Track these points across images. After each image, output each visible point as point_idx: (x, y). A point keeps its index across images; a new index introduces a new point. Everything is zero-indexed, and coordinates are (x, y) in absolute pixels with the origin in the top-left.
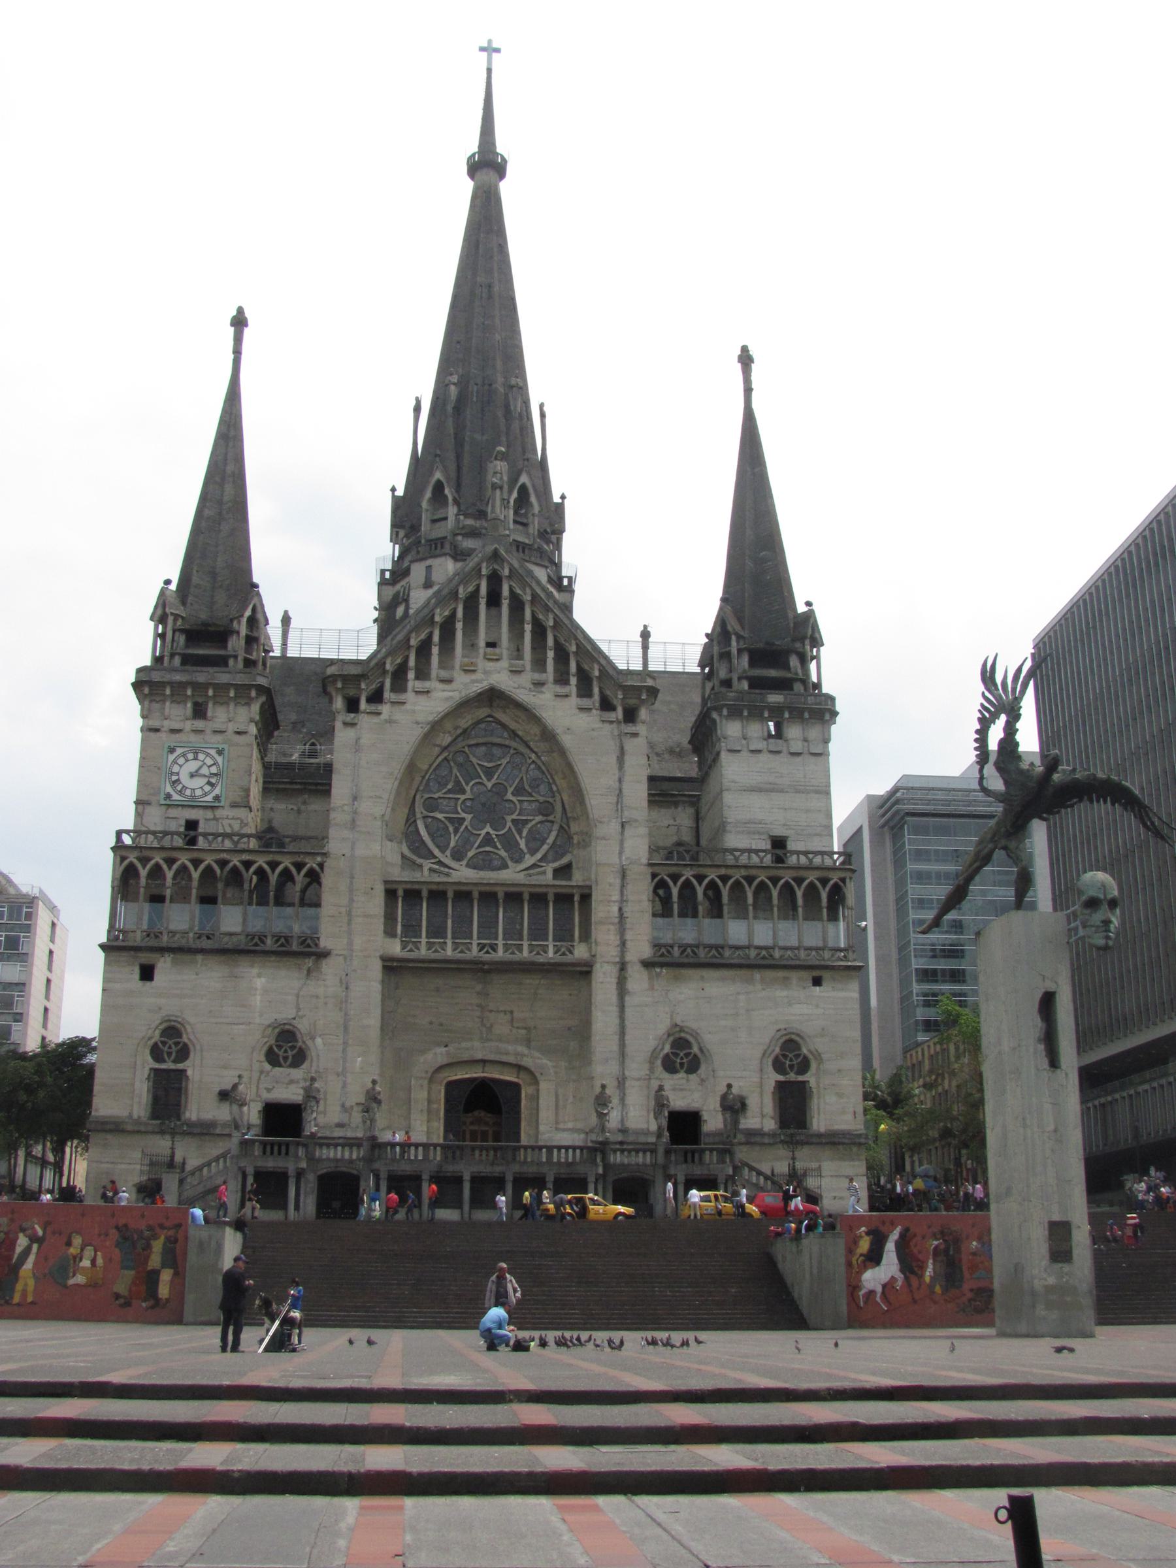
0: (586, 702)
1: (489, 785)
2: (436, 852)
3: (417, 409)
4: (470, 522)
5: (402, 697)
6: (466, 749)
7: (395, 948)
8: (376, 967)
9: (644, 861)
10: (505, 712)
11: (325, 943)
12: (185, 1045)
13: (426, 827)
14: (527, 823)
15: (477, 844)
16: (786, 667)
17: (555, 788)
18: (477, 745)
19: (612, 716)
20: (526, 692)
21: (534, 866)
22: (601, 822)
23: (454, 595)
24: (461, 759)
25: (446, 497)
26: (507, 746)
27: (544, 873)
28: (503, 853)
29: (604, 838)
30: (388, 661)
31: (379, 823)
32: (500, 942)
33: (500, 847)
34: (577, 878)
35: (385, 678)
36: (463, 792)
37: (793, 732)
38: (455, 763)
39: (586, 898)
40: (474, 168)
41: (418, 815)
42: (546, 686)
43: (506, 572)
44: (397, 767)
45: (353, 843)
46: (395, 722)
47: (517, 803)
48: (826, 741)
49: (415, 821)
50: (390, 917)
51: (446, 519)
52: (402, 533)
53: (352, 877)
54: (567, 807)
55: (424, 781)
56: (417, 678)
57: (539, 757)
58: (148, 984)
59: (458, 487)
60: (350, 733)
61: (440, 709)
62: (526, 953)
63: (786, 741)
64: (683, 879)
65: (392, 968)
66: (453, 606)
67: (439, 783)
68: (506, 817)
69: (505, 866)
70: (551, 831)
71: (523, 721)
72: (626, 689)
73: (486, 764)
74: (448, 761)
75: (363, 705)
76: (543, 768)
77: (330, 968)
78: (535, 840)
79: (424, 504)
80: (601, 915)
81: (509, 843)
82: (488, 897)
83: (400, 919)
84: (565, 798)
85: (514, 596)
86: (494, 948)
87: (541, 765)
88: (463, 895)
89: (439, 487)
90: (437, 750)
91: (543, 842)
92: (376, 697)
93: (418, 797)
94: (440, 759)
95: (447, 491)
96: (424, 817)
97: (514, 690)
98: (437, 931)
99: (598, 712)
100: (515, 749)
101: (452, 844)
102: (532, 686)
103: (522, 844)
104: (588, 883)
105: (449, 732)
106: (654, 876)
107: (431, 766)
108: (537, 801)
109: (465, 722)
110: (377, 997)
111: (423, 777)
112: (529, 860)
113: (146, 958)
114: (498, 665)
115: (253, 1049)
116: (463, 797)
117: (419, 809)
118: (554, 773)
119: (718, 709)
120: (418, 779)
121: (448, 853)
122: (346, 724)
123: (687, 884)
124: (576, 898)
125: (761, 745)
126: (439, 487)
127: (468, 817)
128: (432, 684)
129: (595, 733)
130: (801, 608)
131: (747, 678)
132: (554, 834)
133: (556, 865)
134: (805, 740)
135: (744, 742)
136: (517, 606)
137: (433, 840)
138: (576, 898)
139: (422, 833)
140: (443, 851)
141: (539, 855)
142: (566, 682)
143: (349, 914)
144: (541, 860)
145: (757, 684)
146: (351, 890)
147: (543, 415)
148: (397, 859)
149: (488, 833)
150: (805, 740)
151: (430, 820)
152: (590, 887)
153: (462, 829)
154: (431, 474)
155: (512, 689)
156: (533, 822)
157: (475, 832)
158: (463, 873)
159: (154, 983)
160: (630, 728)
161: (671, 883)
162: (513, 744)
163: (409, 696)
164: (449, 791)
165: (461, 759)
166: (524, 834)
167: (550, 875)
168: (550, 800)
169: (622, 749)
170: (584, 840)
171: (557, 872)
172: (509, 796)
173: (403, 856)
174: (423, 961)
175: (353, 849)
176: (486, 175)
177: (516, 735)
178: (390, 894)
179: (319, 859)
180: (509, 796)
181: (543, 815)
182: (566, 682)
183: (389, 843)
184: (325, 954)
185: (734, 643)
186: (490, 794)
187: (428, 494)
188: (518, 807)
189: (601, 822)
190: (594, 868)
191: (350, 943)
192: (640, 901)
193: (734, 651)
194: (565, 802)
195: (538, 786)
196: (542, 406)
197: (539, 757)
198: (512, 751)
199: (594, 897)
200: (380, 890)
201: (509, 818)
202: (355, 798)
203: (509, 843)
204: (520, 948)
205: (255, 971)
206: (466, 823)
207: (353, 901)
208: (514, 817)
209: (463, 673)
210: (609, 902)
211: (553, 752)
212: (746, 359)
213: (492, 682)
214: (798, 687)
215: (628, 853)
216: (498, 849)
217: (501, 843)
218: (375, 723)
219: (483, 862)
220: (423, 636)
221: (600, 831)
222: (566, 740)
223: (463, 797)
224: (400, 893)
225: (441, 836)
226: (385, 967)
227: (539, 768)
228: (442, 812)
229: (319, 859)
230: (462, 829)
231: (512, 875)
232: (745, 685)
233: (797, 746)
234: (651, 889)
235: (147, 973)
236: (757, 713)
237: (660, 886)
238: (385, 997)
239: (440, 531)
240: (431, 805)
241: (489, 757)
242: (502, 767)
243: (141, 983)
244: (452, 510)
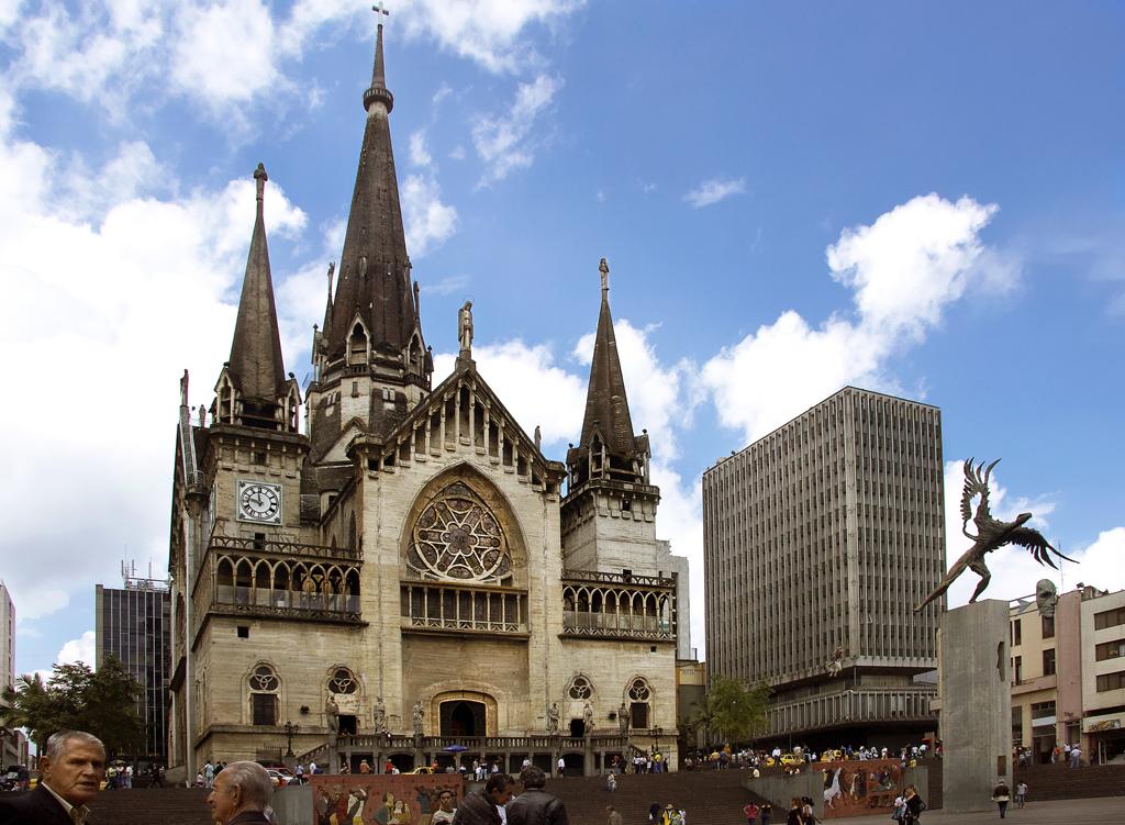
0: (520, 477)
1: (460, 525)
2: (428, 565)
3: (331, 272)
4: (380, 356)
5: (407, 463)
7: (409, 623)
8: (398, 634)
11: (364, 618)
12: (274, 679)
16: (632, 470)
19: (540, 488)
21: (489, 577)
23: (441, 397)
24: (441, 508)
25: (365, 336)
27: (496, 581)
28: (469, 568)
30: (399, 438)
32: (474, 622)
34: (516, 585)
36: (444, 529)
37: (636, 507)
39: (524, 597)
40: (368, 102)
44: (406, 509)
48: (654, 514)
50: (404, 605)
51: (365, 351)
52: (325, 359)
56: (417, 451)
58: (245, 640)
59: (371, 330)
60: (374, 484)
62: (489, 629)
63: (632, 512)
65: (407, 635)
69: (471, 576)
72: (548, 471)
77: (368, 634)
78: (490, 562)
79: (348, 340)
81: (474, 563)
82: (465, 594)
85: (477, 404)
86: (470, 625)
88: (450, 592)
89: (358, 328)
90: (427, 500)
91: (494, 562)
92: (390, 461)
95: (365, 332)
96: (420, 543)
98: (434, 613)
103: (482, 564)
106: (564, 586)
109: (445, 484)
110: (399, 652)
112: (486, 574)
113: (243, 623)
115: (322, 682)
117: (416, 537)
119: (595, 490)
122: (372, 478)
125: (619, 514)
126: (358, 328)
127: (448, 544)
128: (427, 457)
130: (637, 433)
131: (610, 473)
132: (500, 558)
133: (503, 577)
134: (643, 513)
136: (479, 412)
141: (492, 571)
142: (511, 464)
145: (613, 475)
146: (380, 585)
147: (416, 290)
148: (404, 568)
150: (643, 513)
154: (353, 318)
158: (445, 578)
159: (249, 639)
160: (550, 497)
162: (474, 500)
163: (412, 463)
164: (435, 528)
167: (499, 584)
171: (502, 581)
172: (472, 533)
174: (425, 631)
175: (379, 559)
177: (476, 495)
178: (404, 590)
179: (357, 565)
180: (472, 533)
182: (511, 464)
184: (366, 625)
185: (603, 451)
187: (351, 333)
191: (381, 619)
193: (603, 456)
196: (416, 285)
200: (398, 585)
201: (473, 547)
202: (379, 527)
203: (474, 563)
204: (486, 626)
205: (319, 634)
214: (638, 481)
219: (458, 572)
220: (420, 424)
222: (512, 501)
224: (410, 589)
226: (403, 634)
228: (430, 540)
229: (357, 565)
231: (476, 580)
232: (608, 477)
233: (638, 516)
235: (243, 633)
236: (616, 497)
237: (568, 595)
238: (403, 652)
239: (361, 360)
240: (424, 535)
241: (459, 507)
243: (240, 639)
244: (369, 345)
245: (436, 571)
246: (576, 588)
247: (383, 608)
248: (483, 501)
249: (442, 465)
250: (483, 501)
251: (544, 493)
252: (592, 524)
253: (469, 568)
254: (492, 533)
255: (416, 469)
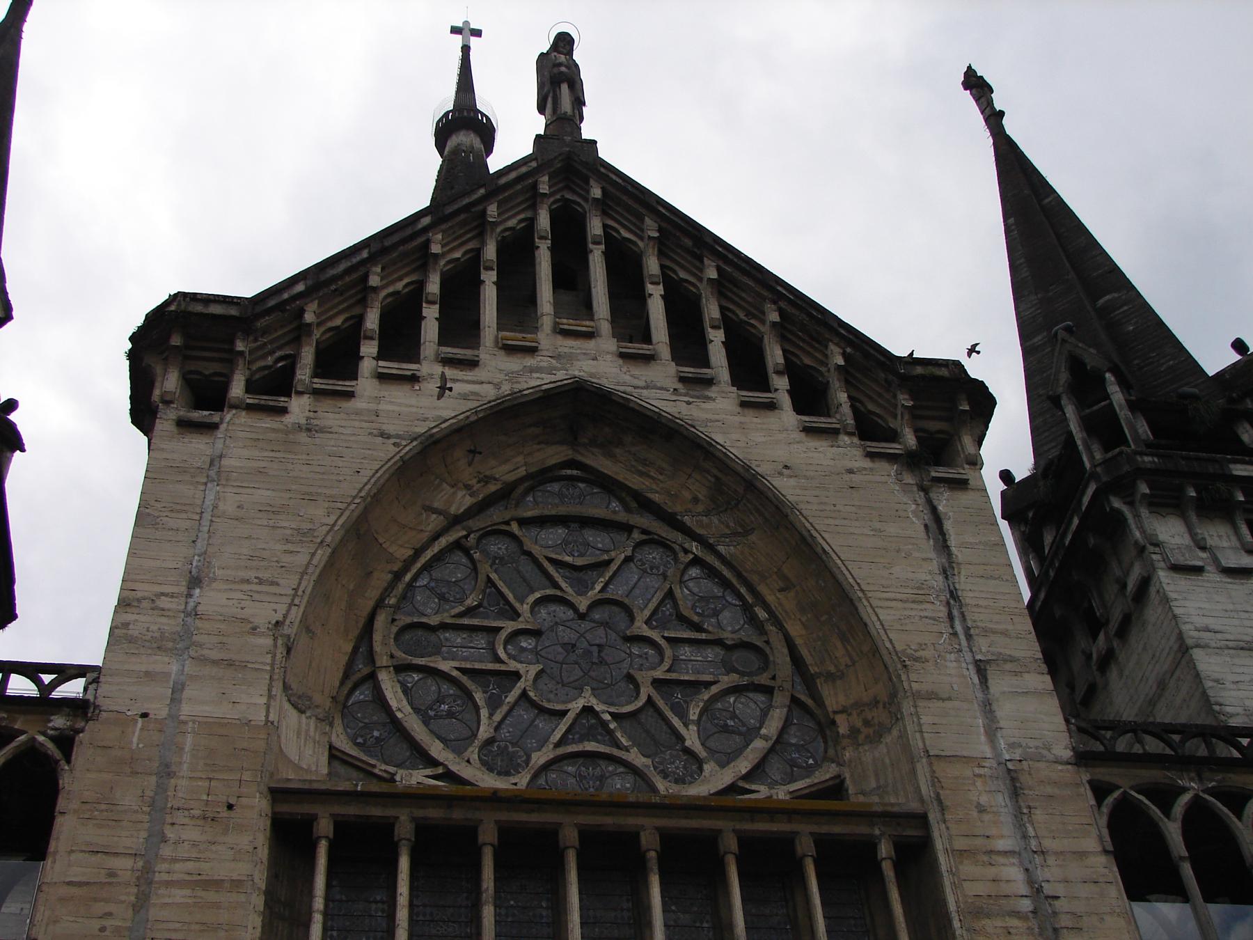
1: (583, 604)
6: (514, 527)
9: (1067, 754)
10: (611, 456)
13: (406, 691)
14: (699, 692)
15: (557, 736)
17: (762, 614)
18: (543, 522)
20: (666, 395)
22: (916, 659)
26: (627, 528)
29: (932, 696)
31: (269, 641)
33: (624, 741)
35: (300, 346)
38: (485, 553)
41: (383, 660)
42: (714, 388)
43: (596, 192)
45: (178, 689)
46: (322, 430)
47: (662, 642)
49: (372, 676)
53: (167, 772)
54: (804, 652)
55: (401, 587)
57: (711, 548)
61: (447, 414)
64: (1186, 798)
66: (470, 246)
67: (442, 598)
68: (639, 676)
70: (765, 714)
71: (661, 471)
73: (568, 559)
74: (467, 552)
75: (237, 389)
76: (727, 573)
80: (972, 889)
83: (319, 903)
84: (795, 630)
87: (717, 564)
90: (435, 522)
91: (751, 733)
93: (381, 620)
94: (443, 542)
97: (636, 392)
99: (856, 440)
100: (644, 532)
101: (484, 732)
102: (679, 386)
104: (914, 806)
105: (468, 487)
106: (1100, 791)
107: (418, 553)
108: (719, 642)
109: (508, 469)
111: (398, 576)
114: (591, 345)
116: (510, 626)
118: (754, 579)
120: (381, 578)
121: (473, 753)
123: (1197, 809)
124: (885, 850)
129: (856, 478)
135: (1204, 555)
137: (426, 723)
138: (885, 850)
139: (393, 704)
140: (457, 746)
141: (743, 766)
143: (145, 880)
144: (747, 777)
149: (588, 710)
151: (416, 677)
152: (922, 819)
153: (512, 697)
155: (629, 389)
156: (714, 689)
157: (546, 705)
161: (1155, 810)
164: (470, 612)
165: (498, 547)
166: (694, 714)
168: (759, 643)
169: (934, 510)
170: (867, 723)
172: (640, 628)
173: (335, 755)
175: (175, 700)
176: (465, 139)
179: (59, 722)
181: (742, 674)
183: (293, 713)
186: (586, 625)
188: (668, 652)
189: (916, 659)
190: (922, 769)
192: (1082, 855)
194: (798, 641)
195: (716, 614)
197: (711, 548)
198: (636, 536)
199: (939, 845)
200: (256, 809)
202: (195, 581)
206: (521, 685)
207: (164, 840)
208: (659, 674)
209: (502, 352)
210: (991, 852)
211: (747, 532)
212: (976, 84)
213: (577, 373)
215: (1009, 730)
216: (618, 745)
217: (630, 738)
218: (274, 430)
221: (919, 680)
222: (787, 488)
223: (510, 626)
224: (325, 827)
225: (450, 714)
227: (712, 573)
229: (59, 722)
230: (512, 697)
234: (1103, 821)
242: (614, 567)
245: (466, 772)
246: (1165, 797)
247: (154, 913)
248: (672, 521)
249: (489, 392)
250: (672, 521)
251: (911, 461)
252: (1153, 613)
253: (636, 757)
254: (730, 625)
255: (378, 399)
